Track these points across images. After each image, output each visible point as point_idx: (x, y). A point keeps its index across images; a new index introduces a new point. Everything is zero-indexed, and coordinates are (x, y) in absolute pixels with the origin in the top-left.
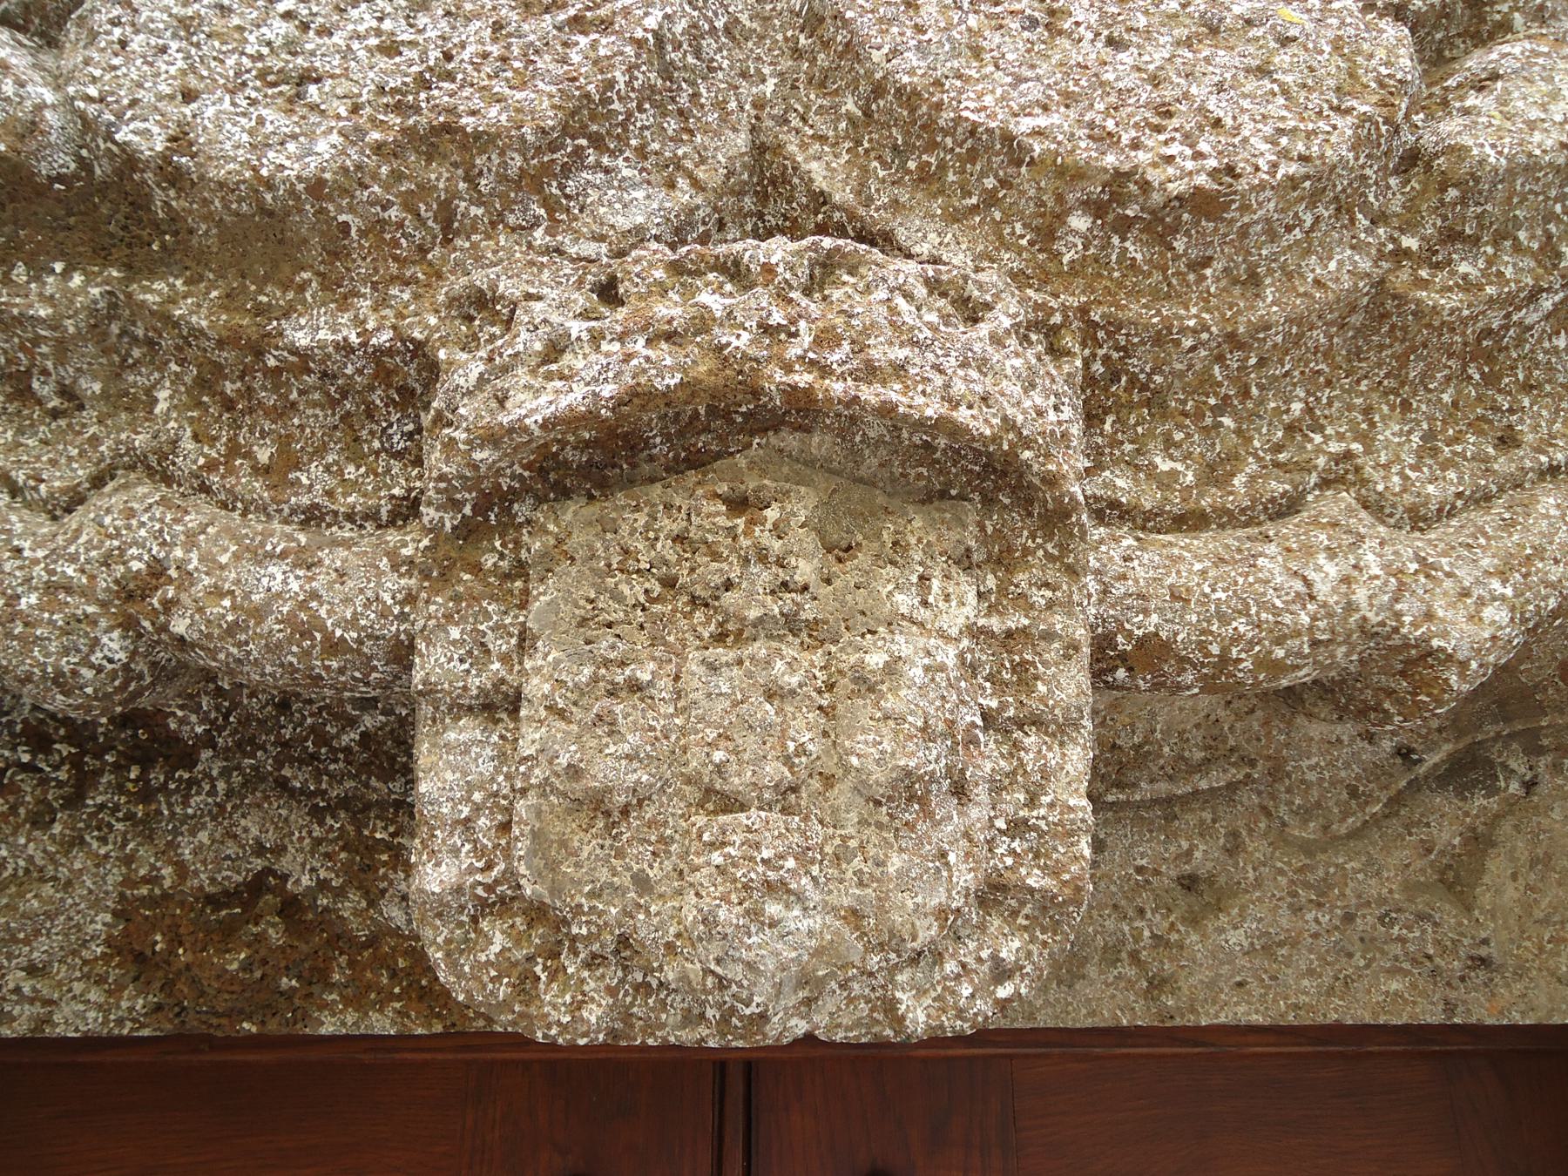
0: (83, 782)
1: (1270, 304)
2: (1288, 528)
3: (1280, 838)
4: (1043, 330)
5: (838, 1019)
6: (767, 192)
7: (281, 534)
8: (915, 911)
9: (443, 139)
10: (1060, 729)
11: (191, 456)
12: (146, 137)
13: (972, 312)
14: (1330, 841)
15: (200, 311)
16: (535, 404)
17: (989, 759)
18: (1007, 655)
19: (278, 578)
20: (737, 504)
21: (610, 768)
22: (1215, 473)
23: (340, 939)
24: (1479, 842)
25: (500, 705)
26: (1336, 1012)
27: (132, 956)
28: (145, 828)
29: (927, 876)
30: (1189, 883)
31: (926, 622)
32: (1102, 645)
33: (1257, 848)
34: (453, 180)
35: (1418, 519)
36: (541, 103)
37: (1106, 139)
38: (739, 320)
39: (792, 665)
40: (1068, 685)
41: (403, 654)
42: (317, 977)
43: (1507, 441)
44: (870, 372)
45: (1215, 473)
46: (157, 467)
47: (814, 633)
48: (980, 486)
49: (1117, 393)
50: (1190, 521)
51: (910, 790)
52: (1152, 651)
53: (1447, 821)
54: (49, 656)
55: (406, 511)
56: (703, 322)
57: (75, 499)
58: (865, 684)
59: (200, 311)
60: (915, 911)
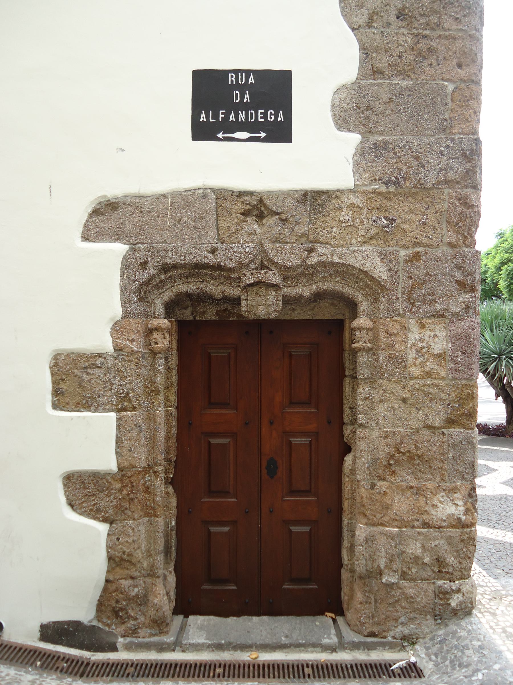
0: (213, 303)
1: (295, 273)
2: (296, 287)
3: (300, 306)
4: (280, 275)
5: (266, 317)
6: (262, 266)
7: (232, 288)
8: (270, 311)
9: (241, 263)
10: (280, 301)
11: (225, 283)
12: (223, 264)
13: (275, 275)
14: (303, 306)
15: (226, 274)
16: (249, 282)
17: (275, 303)
18: (277, 296)
19: (232, 292)
20: (260, 288)
21: (253, 304)
22: (292, 283)
23: (231, 313)
24: (315, 306)
25: (247, 300)
26: (304, 318)
27: (217, 314)
28: (218, 305)
29: (272, 309)
30: (293, 309)
31: (272, 295)
32: (283, 295)
33: (298, 307)
34: (241, 266)
35: (305, 286)
36: (247, 261)
37: (284, 263)
38: (260, 276)
39: (264, 298)
40: (280, 298)
41: (240, 296)
42: (230, 316)
43: (313, 280)
44: (268, 280)
45: (292, 283)
46: (222, 283)
47: (265, 296)
48: (275, 287)
49: (285, 278)
50: (290, 287)
51: (270, 305)
52: (286, 296)
53: (312, 305)
54: (218, 296)
55: (239, 286)
56: (258, 277)
57: (217, 286)
58: (268, 299)
59: (226, 274)
60: (270, 311)
